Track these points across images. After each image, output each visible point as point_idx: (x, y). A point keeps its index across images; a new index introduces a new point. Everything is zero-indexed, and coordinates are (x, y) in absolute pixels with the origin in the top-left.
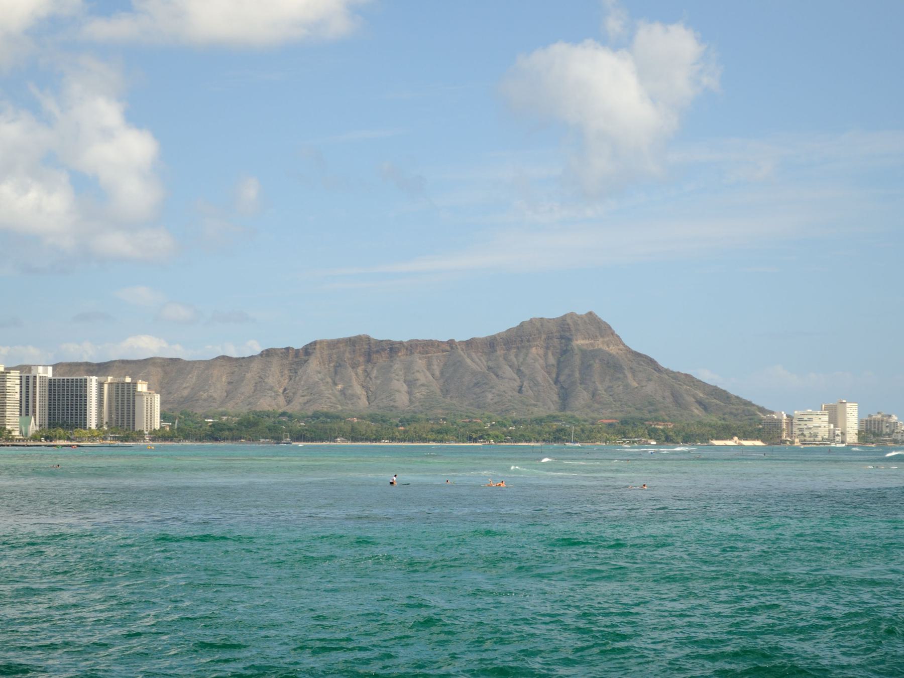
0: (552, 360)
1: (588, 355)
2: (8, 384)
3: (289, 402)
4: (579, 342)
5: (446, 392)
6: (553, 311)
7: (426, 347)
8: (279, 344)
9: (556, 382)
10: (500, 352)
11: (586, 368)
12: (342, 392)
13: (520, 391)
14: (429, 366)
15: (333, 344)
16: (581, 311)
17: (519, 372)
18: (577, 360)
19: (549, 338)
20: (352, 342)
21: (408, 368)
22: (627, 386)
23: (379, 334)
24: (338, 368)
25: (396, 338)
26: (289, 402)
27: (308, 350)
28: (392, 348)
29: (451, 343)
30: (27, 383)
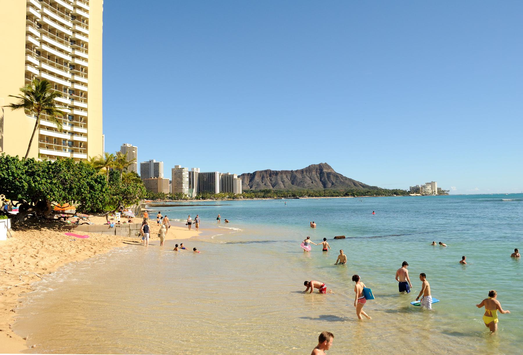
0: (318, 175)
1: (329, 174)
2: (183, 174)
3: (251, 188)
4: (325, 170)
5: (293, 184)
6: (317, 163)
7: (286, 172)
8: (247, 172)
9: (321, 180)
10: (305, 173)
11: (329, 177)
12: (265, 184)
13: (312, 183)
14: (287, 177)
15: (261, 172)
16: (324, 163)
17: (310, 178)
18: (325, 175)
19: (317, 169)
20: (266, 171)
21: (282, 178)
22: (341, 181)
23: (273, 169)
24: (263, 178)
25: (278, 170)
26: (251, 188)
27: (255, 173)
28: (276, 173)
29: (292, 171)
30: (191, 174)
